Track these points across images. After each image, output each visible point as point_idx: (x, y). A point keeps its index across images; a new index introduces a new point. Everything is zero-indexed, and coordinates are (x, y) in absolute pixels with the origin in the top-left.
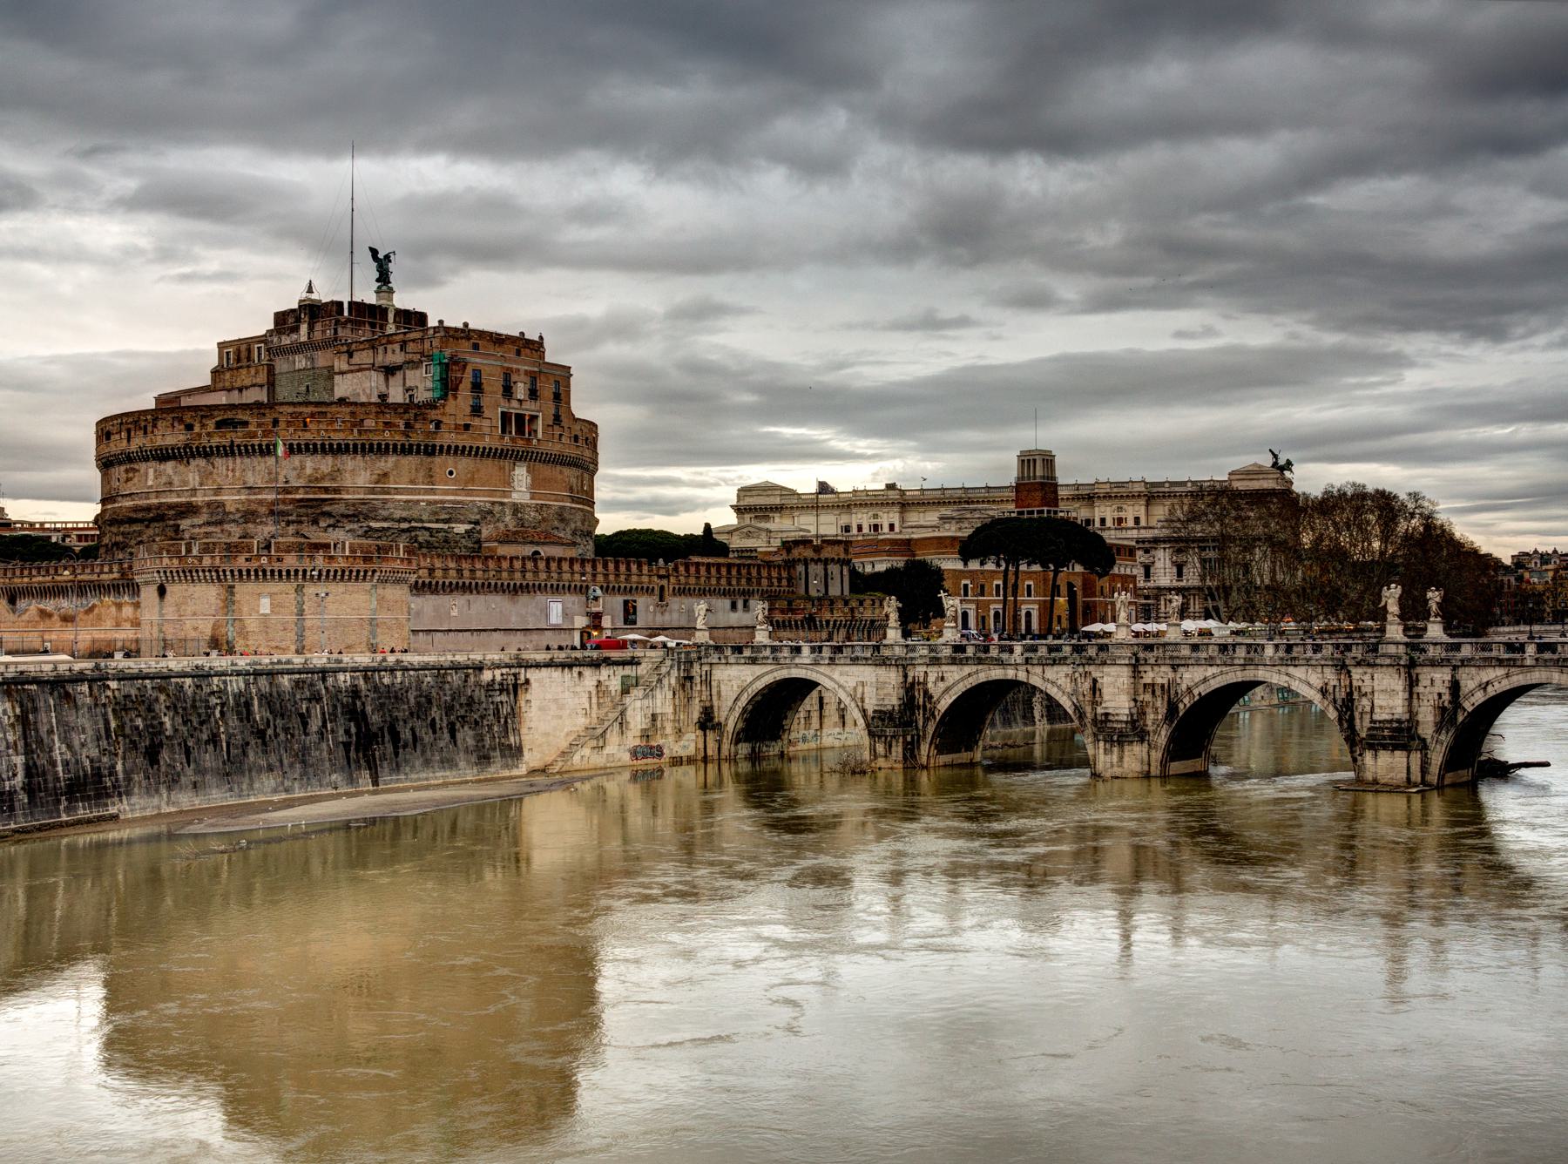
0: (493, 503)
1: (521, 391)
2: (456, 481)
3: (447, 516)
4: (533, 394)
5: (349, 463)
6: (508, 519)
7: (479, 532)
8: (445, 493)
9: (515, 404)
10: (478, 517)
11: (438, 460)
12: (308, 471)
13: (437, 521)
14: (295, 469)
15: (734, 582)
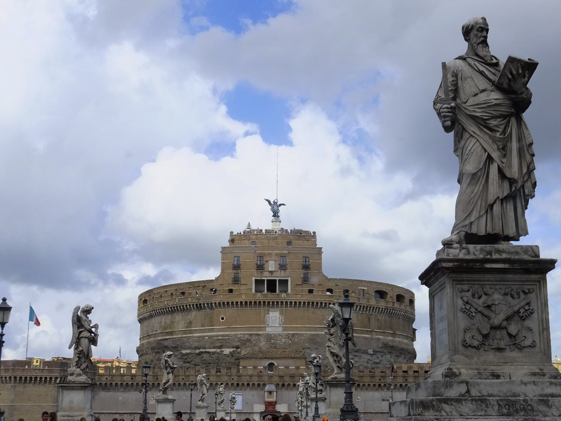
0: (250, 335)
1: (272, 266)
2: (222, 324)
3: (220, 344)
4: (283, 267)
5: (178, 317)
6: (263, 344)
7: (240, 353)
8: (218, 332)
9: (267, 274)
10: (238, 344)
11: (216, 311)
12: (163, 324)
13: (214, 348)
14: (159, 323)
15: (411, 380)
